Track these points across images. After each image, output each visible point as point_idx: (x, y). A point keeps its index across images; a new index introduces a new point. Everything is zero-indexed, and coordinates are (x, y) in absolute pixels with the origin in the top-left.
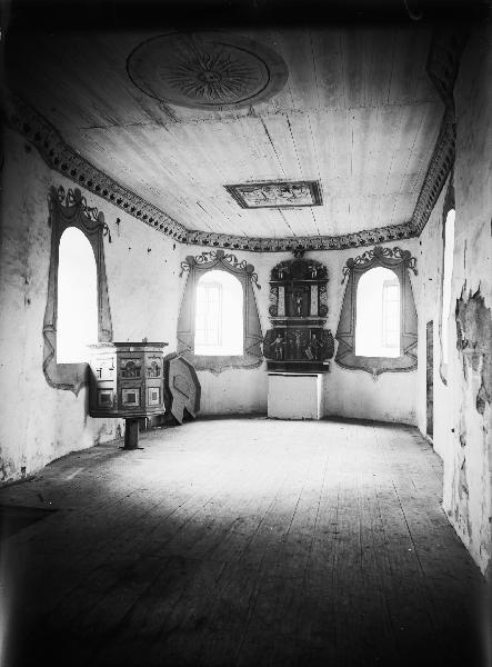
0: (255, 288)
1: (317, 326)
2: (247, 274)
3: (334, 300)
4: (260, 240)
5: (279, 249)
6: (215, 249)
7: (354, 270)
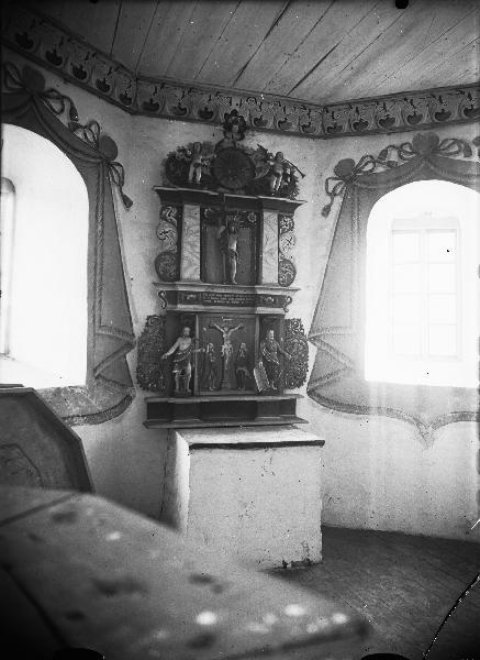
0: (120, 206)
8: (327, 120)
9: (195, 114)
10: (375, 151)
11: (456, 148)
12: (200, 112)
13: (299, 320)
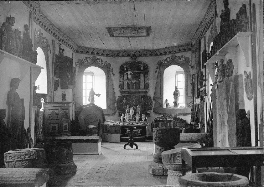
2: (107, 69)
3: (152, 83)
4: (114, 51)
5: (123, 56)
6: (92, 56)
7: (162, 66)
10: (165, 59)
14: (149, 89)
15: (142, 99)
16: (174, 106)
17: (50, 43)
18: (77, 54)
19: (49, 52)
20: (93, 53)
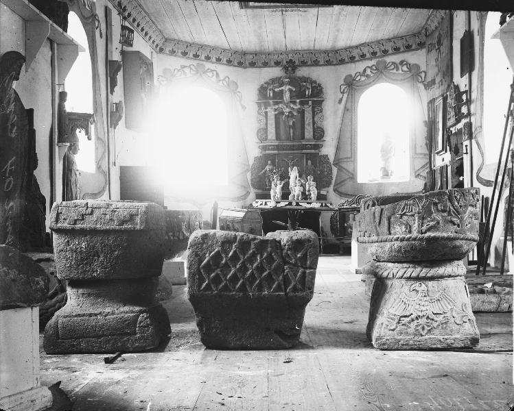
1: (313, 151)
4: (245, 54)
5: (266, 65)
6: (195, 62)
8: (335, 57)
9: (273, 64)
10: (361, 70)
11: (393, 67)
12: (275, 63)
13: (327, 156)
14: (324, 139)
15: (309, 162)
16: (383, 178)
17: (100, 13)
18: (161, 55)
19: (97, 32)
20: (199, 56)
